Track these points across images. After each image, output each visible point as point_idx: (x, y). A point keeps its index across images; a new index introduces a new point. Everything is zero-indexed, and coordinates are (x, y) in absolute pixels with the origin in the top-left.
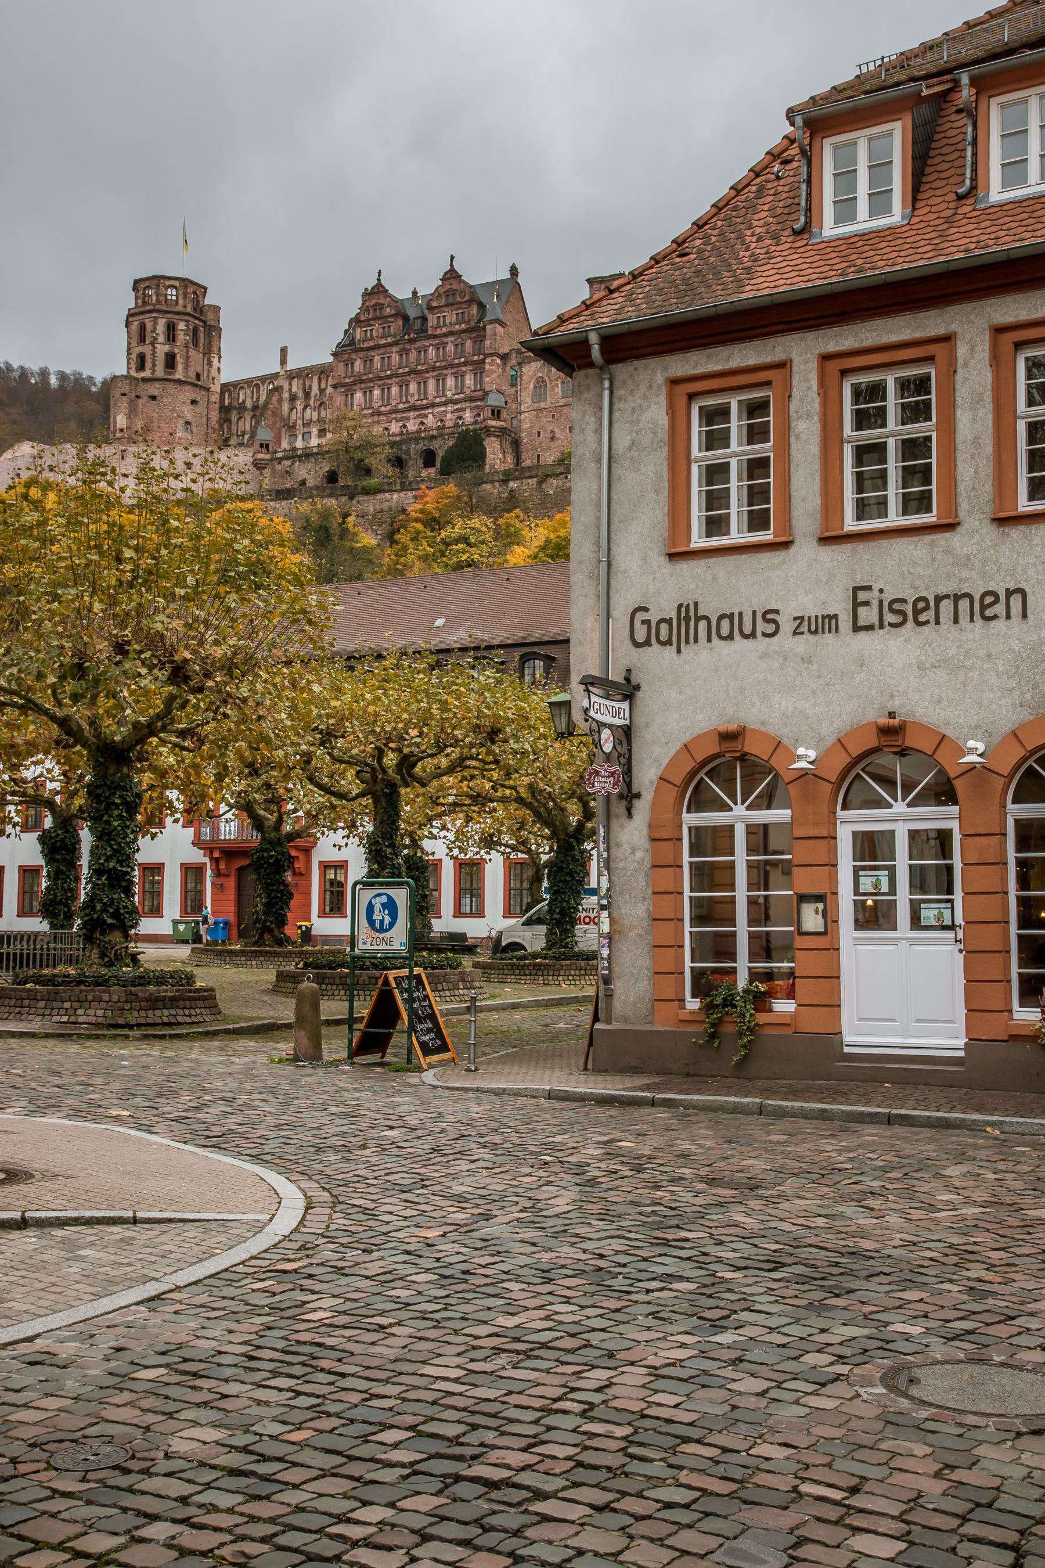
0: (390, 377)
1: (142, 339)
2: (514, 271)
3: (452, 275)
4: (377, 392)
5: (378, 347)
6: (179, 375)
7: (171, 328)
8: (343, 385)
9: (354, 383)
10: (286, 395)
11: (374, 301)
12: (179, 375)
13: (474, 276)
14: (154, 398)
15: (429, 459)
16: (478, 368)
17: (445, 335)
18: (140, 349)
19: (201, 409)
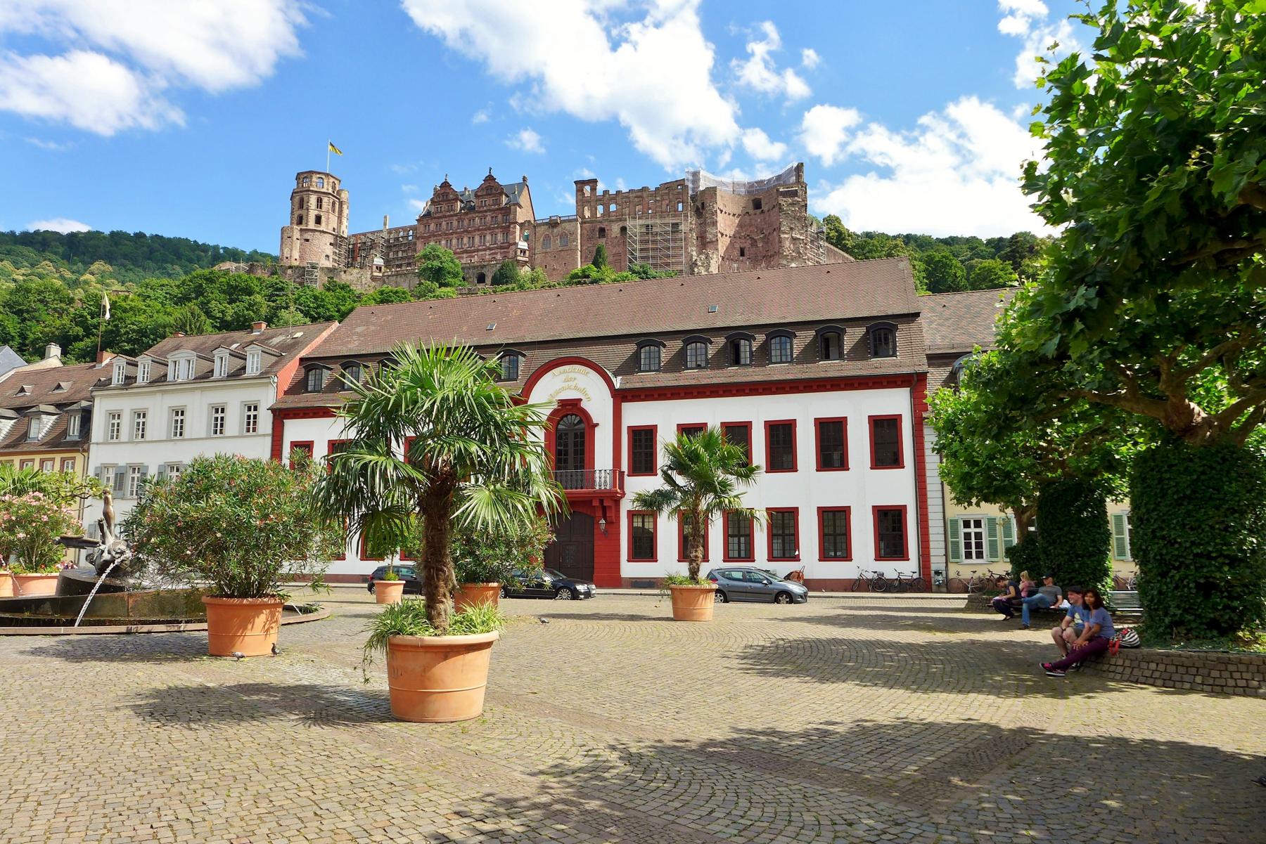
1: (301, 207)
2: (524, 179)
3: (490, 178)
6: (323, 227)
7: (319, 201)
12: (323, 227)
13: (502, 180)
15: (481, 279)
16: (507, 230)
18: (300, 212)
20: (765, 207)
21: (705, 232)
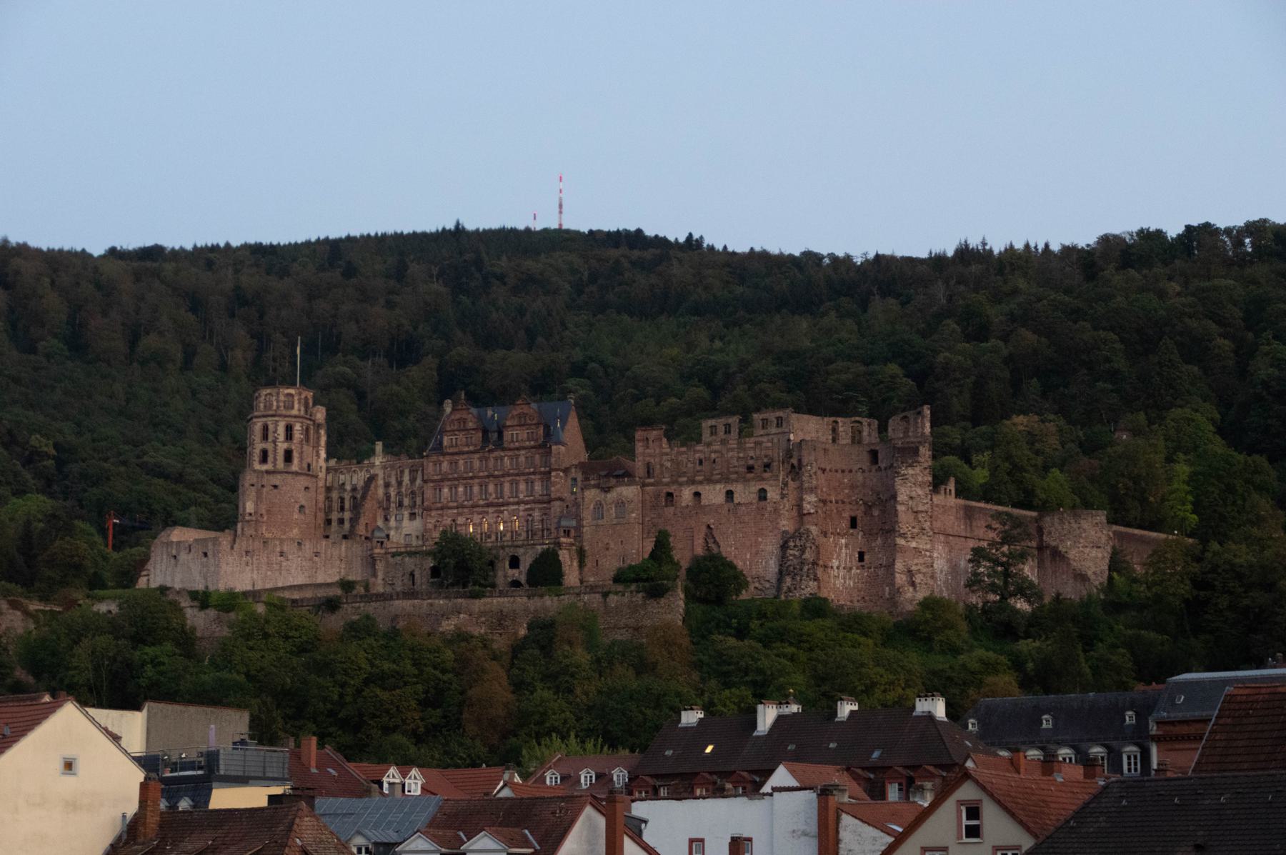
0: (471, 478)
1: (265, 437)
4: (461, 489)
5: (463, 453)
6: (295, 466)
7: (289, 429)
8: (433, 481)
9: (442, 480)
10: (381, 482)
11: (458, 416)
14: (275, 487)
17: (518, 449)
18: (263, 445)
21: (802, 499)
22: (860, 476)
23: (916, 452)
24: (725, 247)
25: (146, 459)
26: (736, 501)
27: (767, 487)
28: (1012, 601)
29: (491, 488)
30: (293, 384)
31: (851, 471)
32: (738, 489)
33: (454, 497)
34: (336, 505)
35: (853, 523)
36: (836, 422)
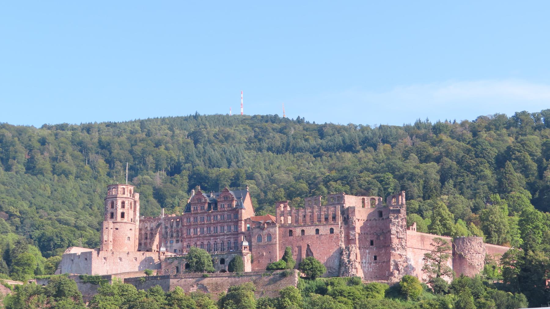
1: (112, 207)
4: (199, 230)
6: (125, 220)
7: (123, 203)
10: (163, 226)
14: (117, 229)
19: (133, 231)
20: (384, 217)
21: (349, 233)
22: (374, 223)
23: (399, 212)
24: (314, 122)
25: (60, 217)
26: (320, 234)
27: (334, 228)
28: (442, 277)
29: (212, 229)
30: (125, 184)
31: (370, 220)
32: (321, 228)
33: (195, 233)
34: (143, 237)
35: (372, 243)
36: (363, 199)
